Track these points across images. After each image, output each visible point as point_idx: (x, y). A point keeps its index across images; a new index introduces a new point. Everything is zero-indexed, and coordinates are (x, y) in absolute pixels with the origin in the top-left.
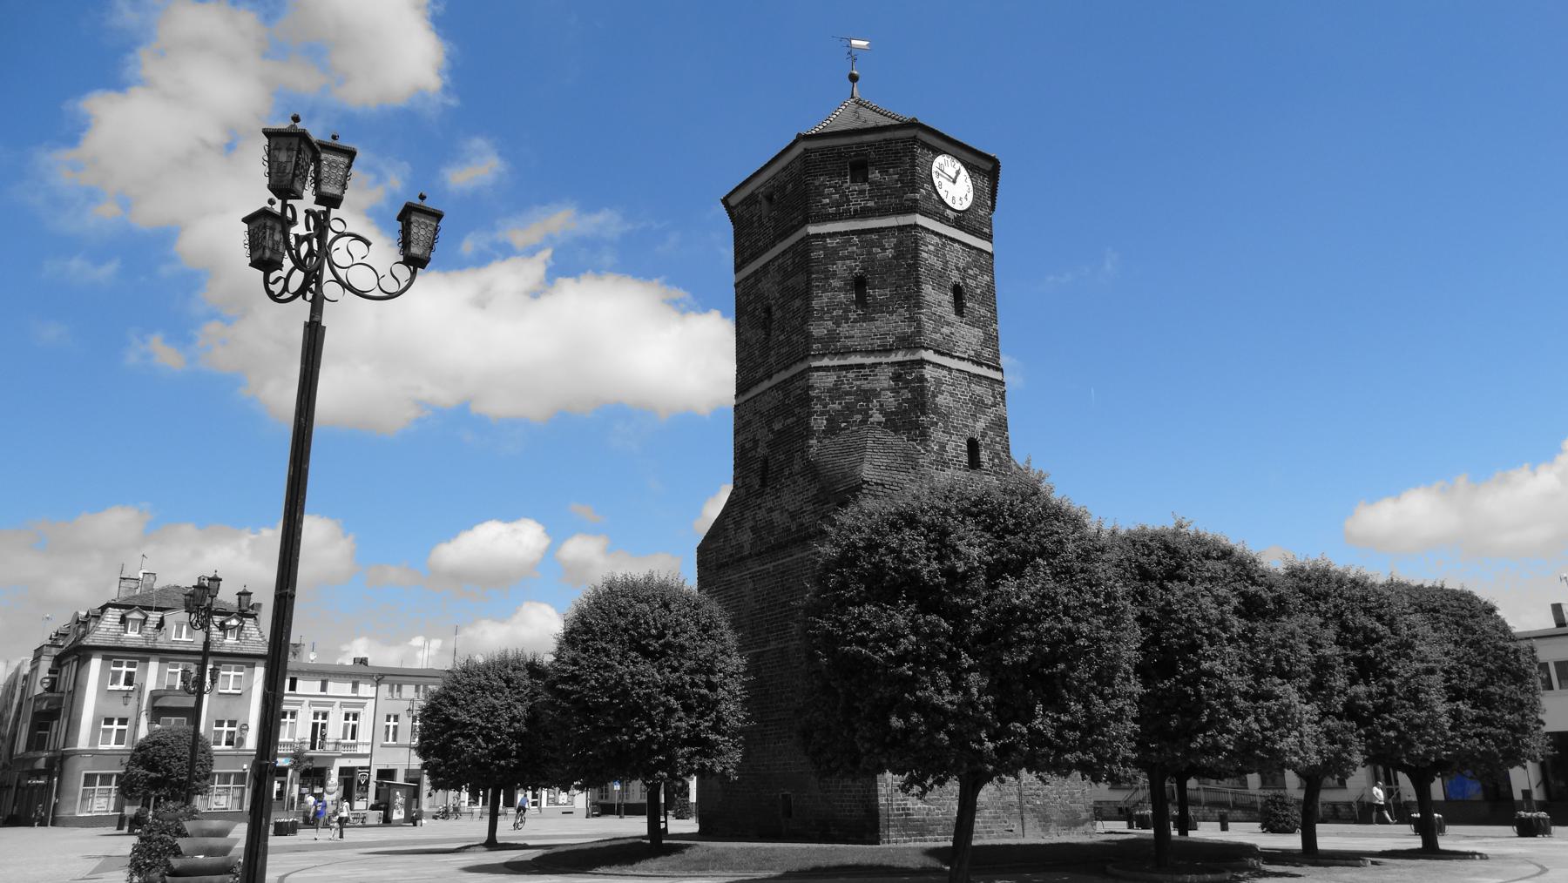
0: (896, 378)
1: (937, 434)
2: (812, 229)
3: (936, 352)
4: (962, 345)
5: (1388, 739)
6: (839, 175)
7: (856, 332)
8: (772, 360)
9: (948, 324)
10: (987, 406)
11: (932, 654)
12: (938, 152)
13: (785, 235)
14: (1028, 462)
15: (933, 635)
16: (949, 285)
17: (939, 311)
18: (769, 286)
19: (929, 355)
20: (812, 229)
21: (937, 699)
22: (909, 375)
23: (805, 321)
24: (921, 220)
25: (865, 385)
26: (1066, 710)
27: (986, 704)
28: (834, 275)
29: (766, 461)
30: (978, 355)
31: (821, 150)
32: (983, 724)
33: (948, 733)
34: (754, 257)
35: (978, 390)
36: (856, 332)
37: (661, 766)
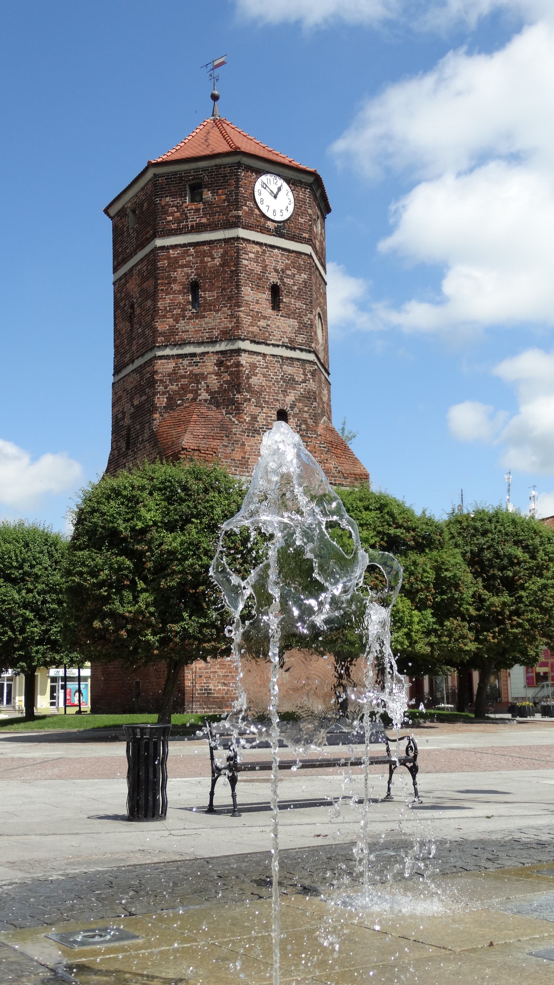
0: (220, 364)
1: (250, 408)
2: (159, 242)
3: (253, 342)
4: (277, 334)
5: (515, 635)
6: (181, 196)
7: (190, 327)
8: (134, 348)
9: (265, 318)
10: (297, 383)
11: (119, 580)
12: (260, 172)
13: (142, 246)
14: (344, 424)
15: (120, 569)
16: (268, 285)
17: (257, 308)
18: (133, 287)
19: (246, 345)
20: (159, 242)
21: (121, 610)
22: (228, 362)
23: (153, 319)
24: (242, 233)
25: (196, 370)
26: (205, 616)
27: (152, 614)
28: (175, 280)
29: (129, 430)
30: (291, 341)
31: (168, 176)
32: (149, 625)
33: (127, 631)
34: (125, 261)
35: (289, 370)
36: (190, 327)
37: (21, 658)
